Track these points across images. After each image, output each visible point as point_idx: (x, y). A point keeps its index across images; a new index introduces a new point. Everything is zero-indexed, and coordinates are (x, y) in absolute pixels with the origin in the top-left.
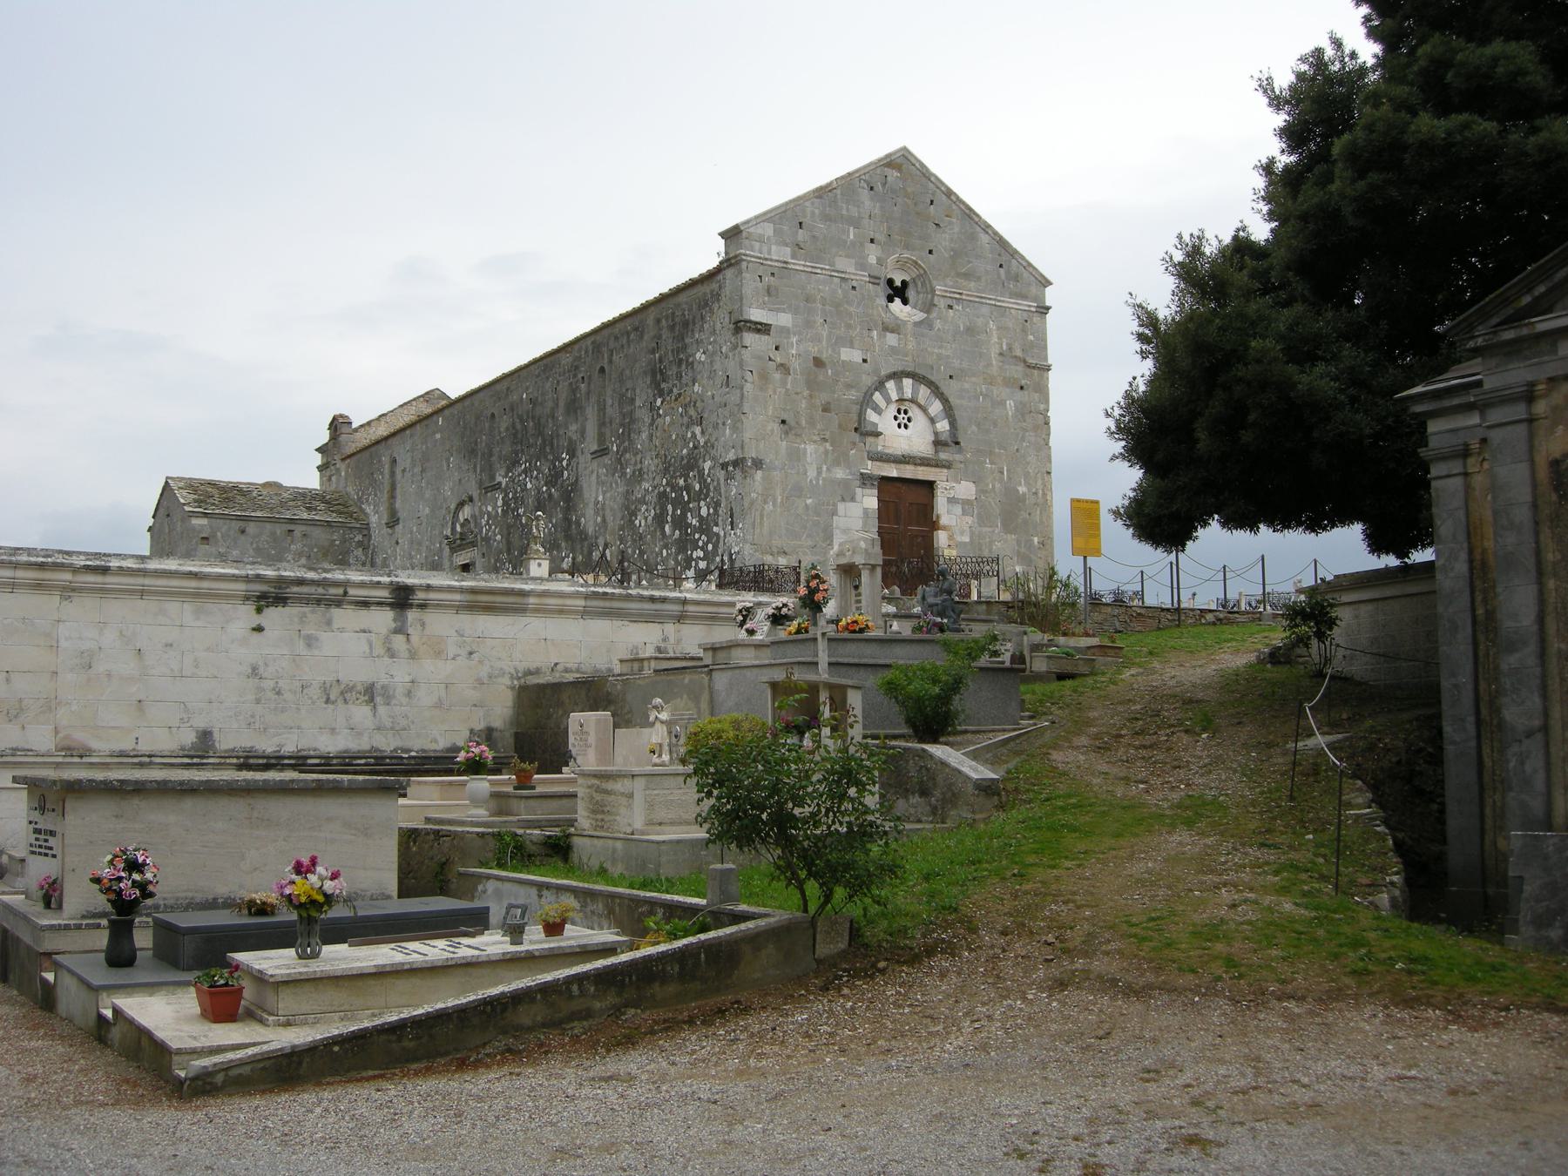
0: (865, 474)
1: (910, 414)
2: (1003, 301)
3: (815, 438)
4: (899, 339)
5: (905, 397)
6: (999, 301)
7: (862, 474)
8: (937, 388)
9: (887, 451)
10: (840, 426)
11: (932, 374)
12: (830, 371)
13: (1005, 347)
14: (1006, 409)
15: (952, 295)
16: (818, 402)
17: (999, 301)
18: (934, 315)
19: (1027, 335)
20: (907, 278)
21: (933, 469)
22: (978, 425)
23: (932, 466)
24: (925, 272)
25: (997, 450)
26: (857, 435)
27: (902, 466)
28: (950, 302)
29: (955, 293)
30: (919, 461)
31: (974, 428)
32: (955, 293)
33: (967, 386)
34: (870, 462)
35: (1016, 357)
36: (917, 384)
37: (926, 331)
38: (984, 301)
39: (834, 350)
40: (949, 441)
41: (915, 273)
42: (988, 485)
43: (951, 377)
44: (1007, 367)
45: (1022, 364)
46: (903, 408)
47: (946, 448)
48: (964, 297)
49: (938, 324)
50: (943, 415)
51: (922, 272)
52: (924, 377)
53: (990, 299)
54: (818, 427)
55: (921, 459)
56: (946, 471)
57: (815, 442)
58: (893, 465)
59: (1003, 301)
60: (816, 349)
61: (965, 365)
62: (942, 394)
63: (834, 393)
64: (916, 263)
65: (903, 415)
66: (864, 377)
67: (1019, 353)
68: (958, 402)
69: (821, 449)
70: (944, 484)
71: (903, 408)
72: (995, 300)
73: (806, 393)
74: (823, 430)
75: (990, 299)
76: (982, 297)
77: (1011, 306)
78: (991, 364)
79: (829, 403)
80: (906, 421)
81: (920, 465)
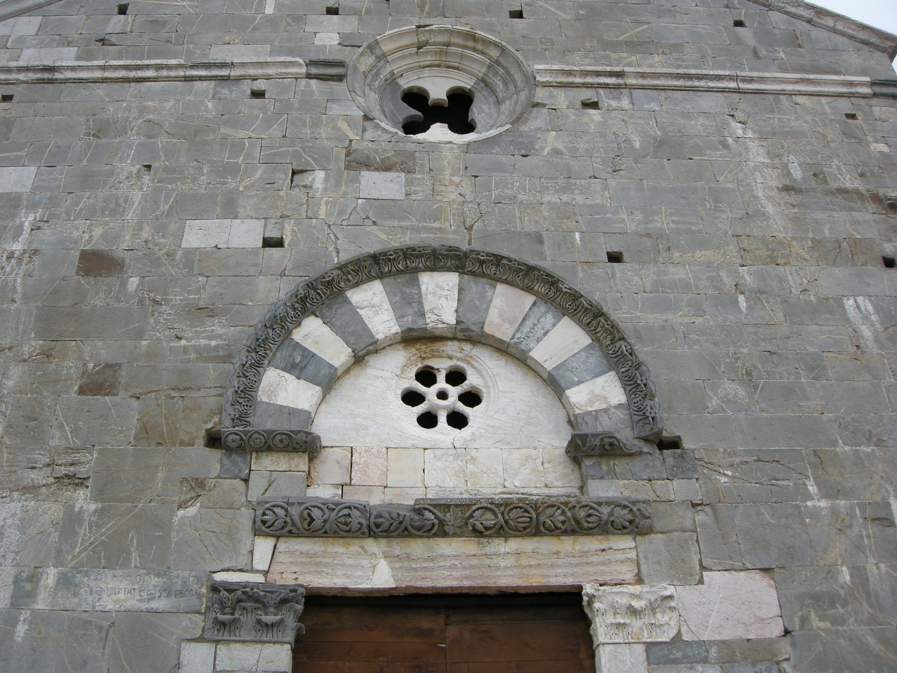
0: (230, 588)
1: (473, 380)
2: (762, 80)
3: (37, 477)
4: (408, 183)
5: (431, 321)
6: (751, 80)
7: (215, 588)
8: (552, 281)
9: (353, 497)
10: (146, 431)
11: (542, 255)
12: (134, 282)
13: (797, 173)
14: (847, 320)
15: (589, 80)
16: (70, 367)
17: (751, 80)
18: (537, 121)
19: (861, 141)
20: (466, 82)
21: (567, 544)
22: (749, 378)
23: (553, 531)
24: (503, 49)
25: (843, 448)
26: (215, 455)
27: (418, 547)
28: (588, 95)
29: (598, 74)
30: (489, 519)
31: (734, 389)
32: (598, 74)
33: (678, 273)
34: (263, 547)
35: (842, 191)
36: (475, 286)
37: (506, 159)
38: (696, 83)
39: (160, 229)
40: (627, 436)
41: (478, 65)
42: (831, 573)
43: (615, 258)
44: (820, 216)
45: (872, 207)
46: (442, 366)
47: (620, 465)
48: (632, 81)
49: (552, 140)
50: (595, 360)
51: (495, 53)
52: (498, 260)
53: (719, 78)
54: (56, 440)
55: (507, 505)
56: (625, 543)
57: (31, 489)
58: (371, 545)
59: (762, 80)
60: (98, 232)
61: (662, 222)
62: (575, 296)
63: (139, 334)
64: (473, 37)
65: (430, 392)
66: (263, 283)
67: (849, 181)
68: (654, 318)
69: (53, 511)
70: (622, 596)
71: (442, 366)
72: (731, 78)
73: (32, 345)
74: (70, 450)
75: (719, 78)
76: (690, 77)
77: (789, 87)
78: (764, 216)
79: (113, 367)
80: (454, 392)
81: (502, 531)
